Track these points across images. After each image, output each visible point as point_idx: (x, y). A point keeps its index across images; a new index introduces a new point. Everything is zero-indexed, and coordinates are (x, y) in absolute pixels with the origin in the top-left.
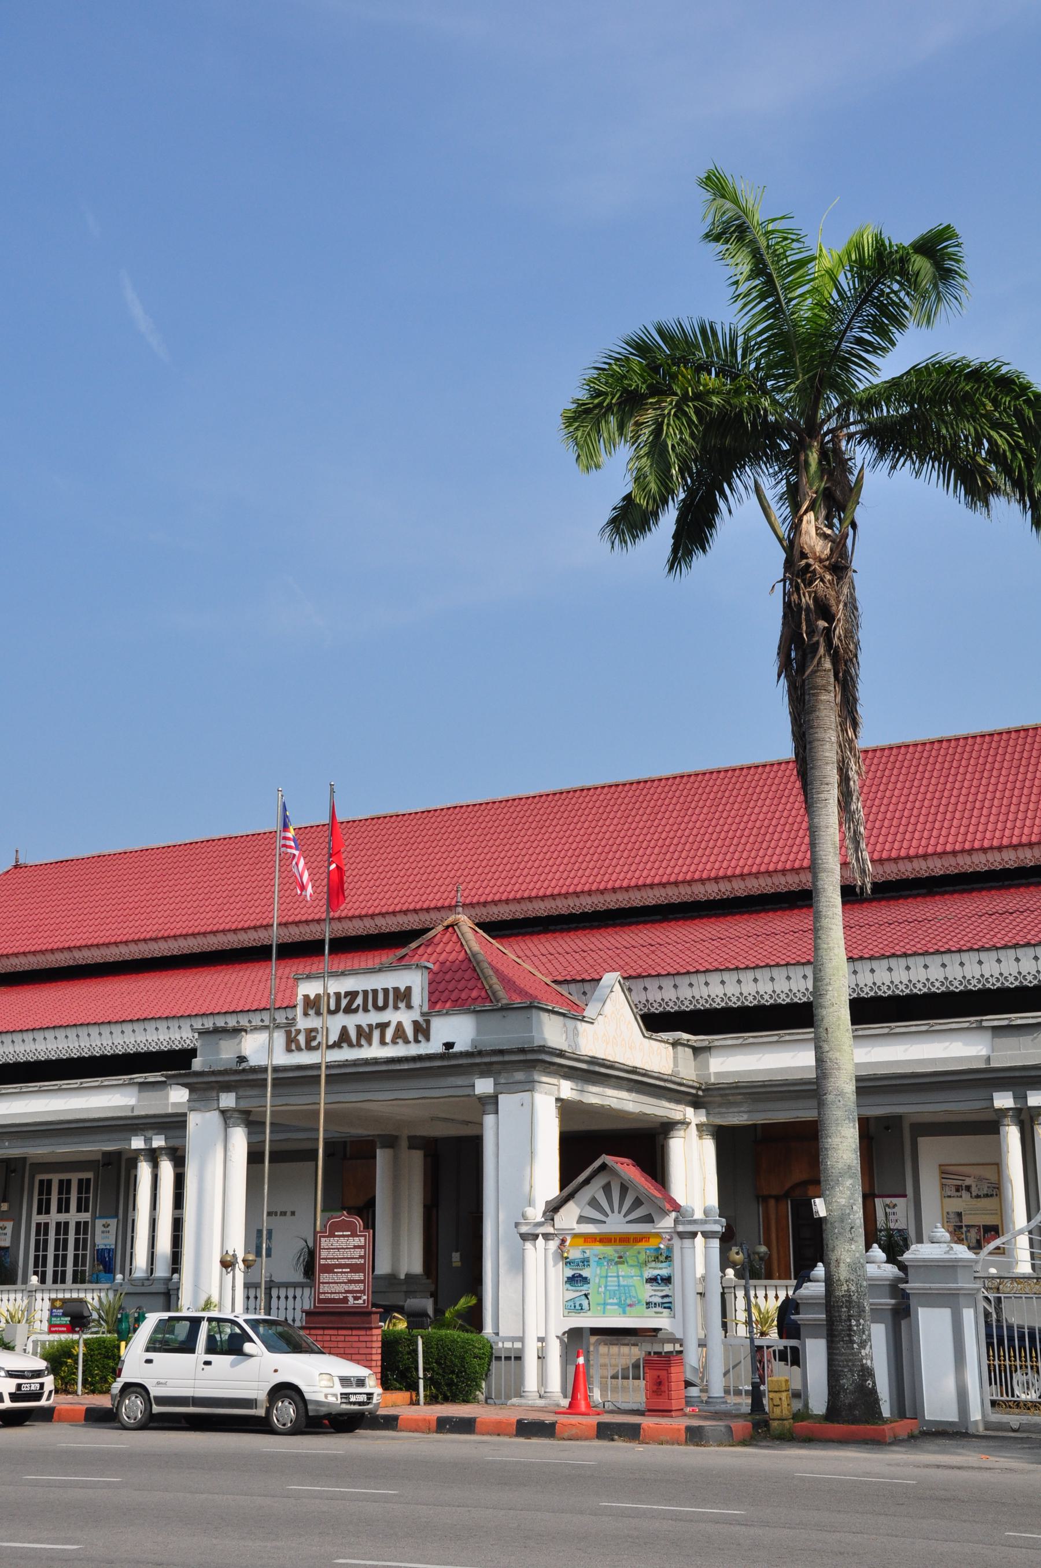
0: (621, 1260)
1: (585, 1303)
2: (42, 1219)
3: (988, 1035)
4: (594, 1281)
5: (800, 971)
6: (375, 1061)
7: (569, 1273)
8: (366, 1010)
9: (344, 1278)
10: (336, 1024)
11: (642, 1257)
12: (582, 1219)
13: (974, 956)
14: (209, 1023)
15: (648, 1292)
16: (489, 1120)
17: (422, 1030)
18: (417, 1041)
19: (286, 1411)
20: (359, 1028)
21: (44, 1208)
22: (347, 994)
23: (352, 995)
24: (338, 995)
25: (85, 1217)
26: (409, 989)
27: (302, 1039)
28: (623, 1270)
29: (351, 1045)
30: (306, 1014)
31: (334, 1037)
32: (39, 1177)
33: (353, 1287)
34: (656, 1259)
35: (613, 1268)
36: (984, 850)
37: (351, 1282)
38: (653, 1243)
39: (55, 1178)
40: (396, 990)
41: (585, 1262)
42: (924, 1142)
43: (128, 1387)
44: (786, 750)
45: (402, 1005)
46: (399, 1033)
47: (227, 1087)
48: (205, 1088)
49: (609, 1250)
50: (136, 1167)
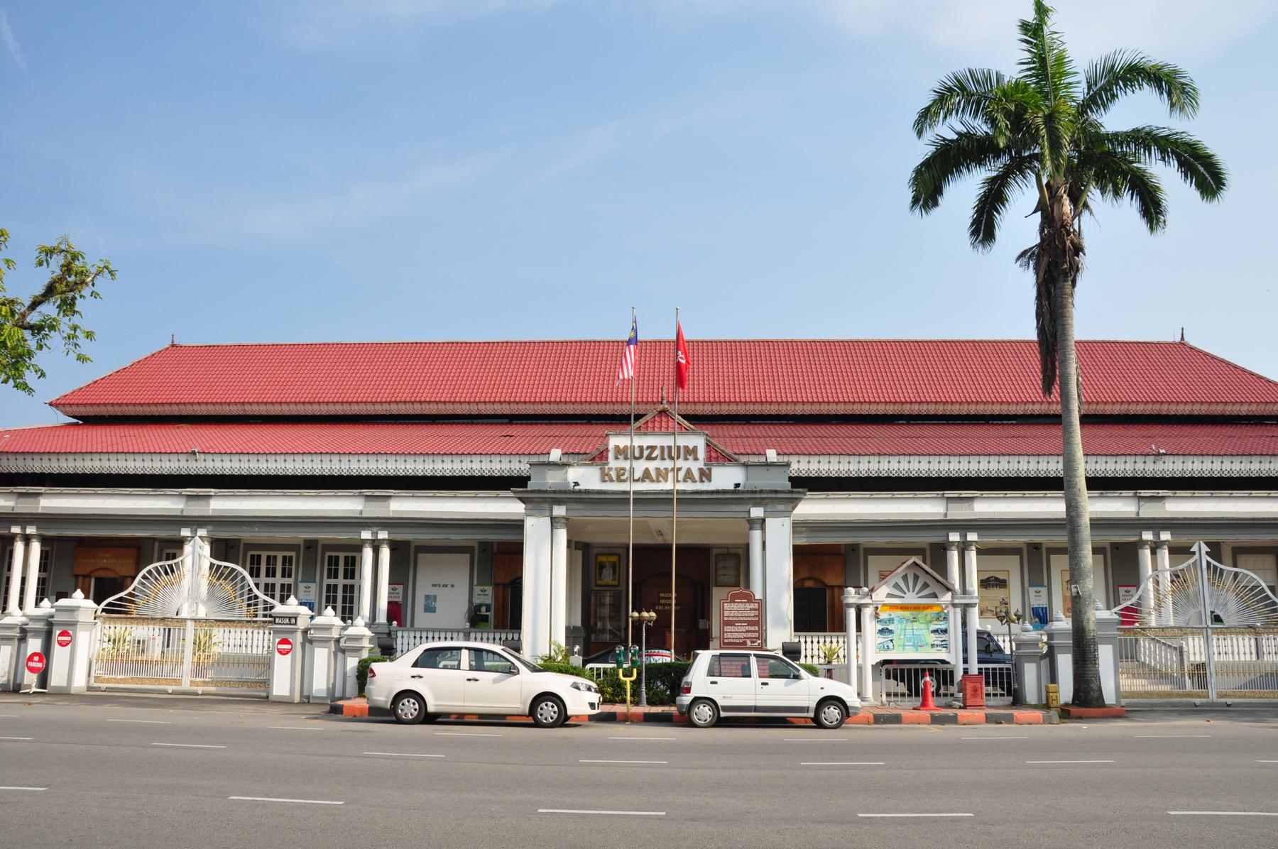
0: (915, 620)
1: (891, 645)
2: (332, 581)
3: (944, 502)
4: (897, 632)
5: (1055, 458)
6: (613, 493)
7: (880, 627)
8: (663, 459)
9: (743, 629)
10: (640, 466)
11: (929, 618)
12: (889, 595)
13: (488, 458)
14: (535, 459)
15: (932, 638)
16: (756, 535)
17: (705, 475)
18: (702, 481)
19: (832, 713)
20: (658, 469)
21: (333, 574)
22: (648, 447)
23: (652, 448)
24: (641, 448)
25: (287, 581)
26: (695, 448)
27: (613, 474)
28: (916, 625)
29: (652, 481)
30: (616, 458)
31: (638, 475)
32: (250, 553)
33: (750, 635)
34: (938, 619)
35: (909, 626)
36: (500, 402)
37: (748, 632)
38: (936, 610)
39: (264, 555)
40: (686, 448)
41: (891, 621)
42: (421, 556)
43: (696, 700)
44: (1028, 330)
45: (691, 458)
46: (689, 476)
47: (559, 502)
48: (541, 500)
49: (907, 614)
50: (12, 544)
